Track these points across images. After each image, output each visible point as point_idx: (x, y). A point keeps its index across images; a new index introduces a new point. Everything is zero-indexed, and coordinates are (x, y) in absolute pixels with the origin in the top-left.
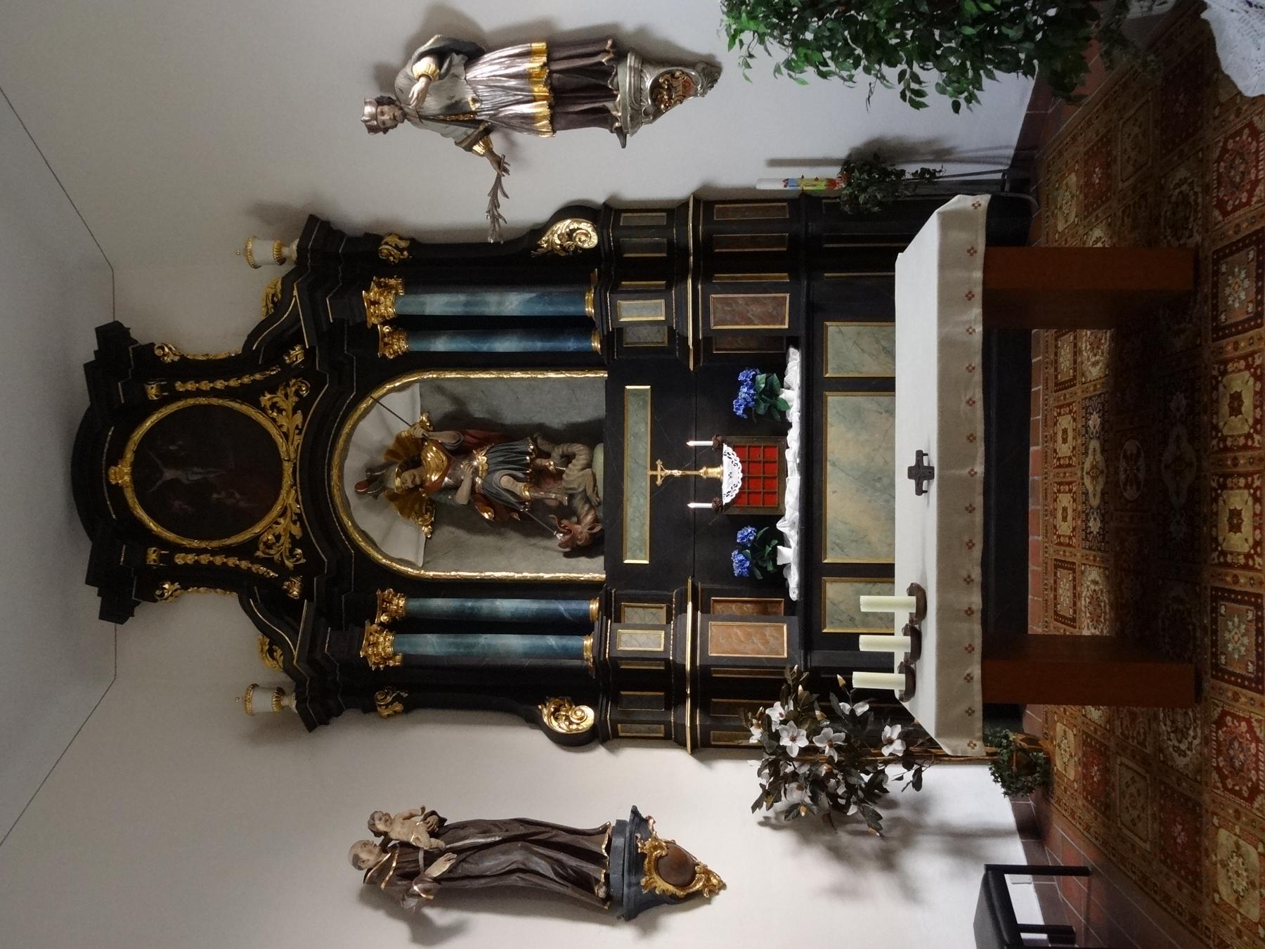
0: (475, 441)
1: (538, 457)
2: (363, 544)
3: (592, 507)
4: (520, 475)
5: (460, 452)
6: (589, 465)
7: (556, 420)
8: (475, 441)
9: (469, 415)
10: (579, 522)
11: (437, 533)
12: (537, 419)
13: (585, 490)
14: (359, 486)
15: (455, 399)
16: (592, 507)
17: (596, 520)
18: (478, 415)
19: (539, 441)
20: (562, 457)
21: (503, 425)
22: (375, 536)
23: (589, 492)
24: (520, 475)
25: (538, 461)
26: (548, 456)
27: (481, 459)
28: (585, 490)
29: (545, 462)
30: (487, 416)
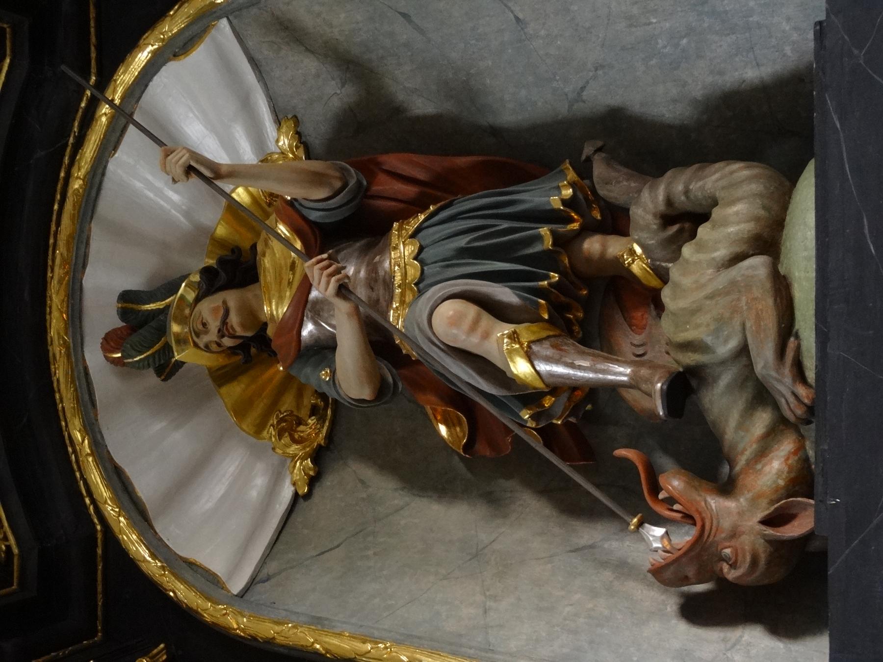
0: (410, 191)
1: (590, 229)
2: (110, 510)
3: (781, 424)
4: (504, 294)
5: (349, 228)
6: (768, 242)
7: (663, 95)
8: (410, 191)
9: (397, 111)
10: (727, 488)
11: (329, 481)
12: (601, 95)
13: (744, 351)
14: (111, 342)
15: (351, 64)
16: (781, 424)
17: (802, 482)
18: (422, 106)
19: (599, 169)
20: (667, 219)
21: (495, 132)
22: (146, 486)
23: (764, 357)
24: (504, 294)
25: (593, 245)
26: (616, 222)
27: (401, 254)
28: (744, 351)
29: (615, 246)
30: (448, 107)
